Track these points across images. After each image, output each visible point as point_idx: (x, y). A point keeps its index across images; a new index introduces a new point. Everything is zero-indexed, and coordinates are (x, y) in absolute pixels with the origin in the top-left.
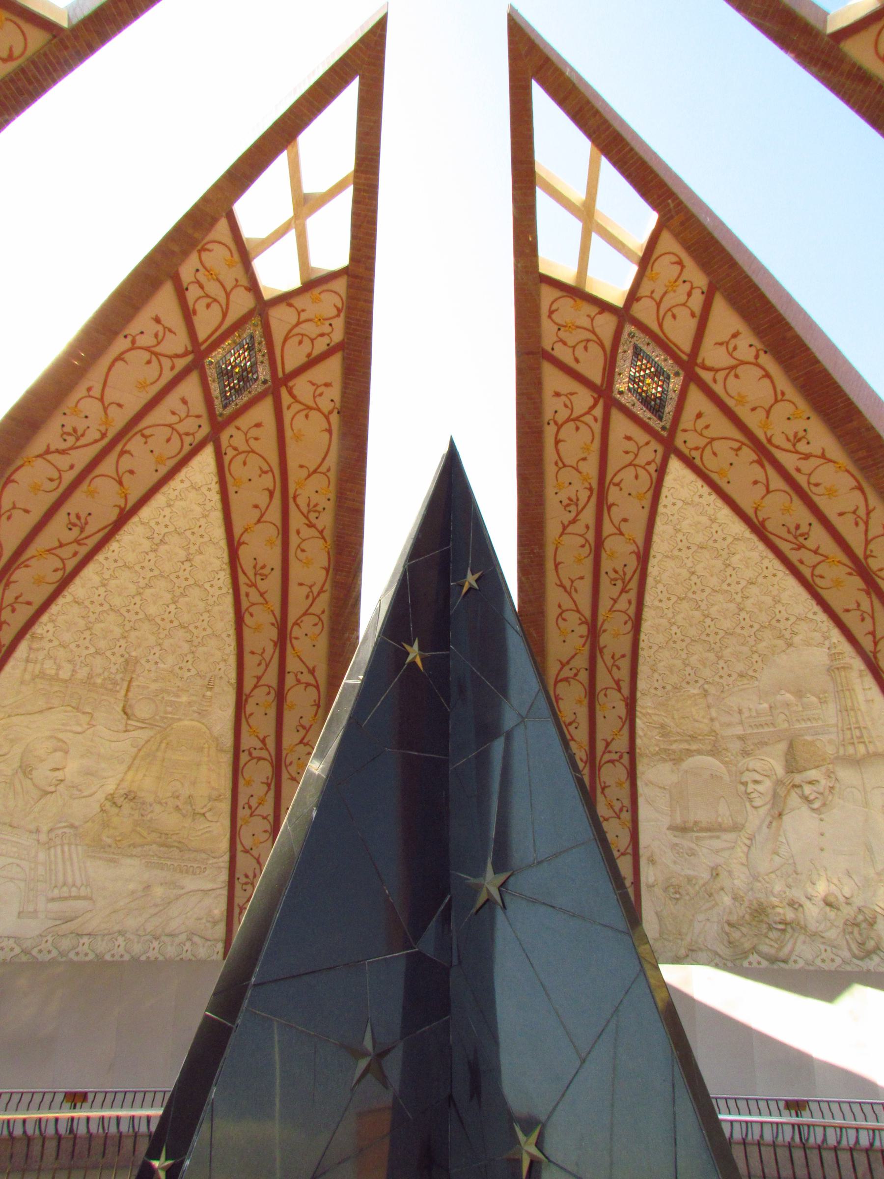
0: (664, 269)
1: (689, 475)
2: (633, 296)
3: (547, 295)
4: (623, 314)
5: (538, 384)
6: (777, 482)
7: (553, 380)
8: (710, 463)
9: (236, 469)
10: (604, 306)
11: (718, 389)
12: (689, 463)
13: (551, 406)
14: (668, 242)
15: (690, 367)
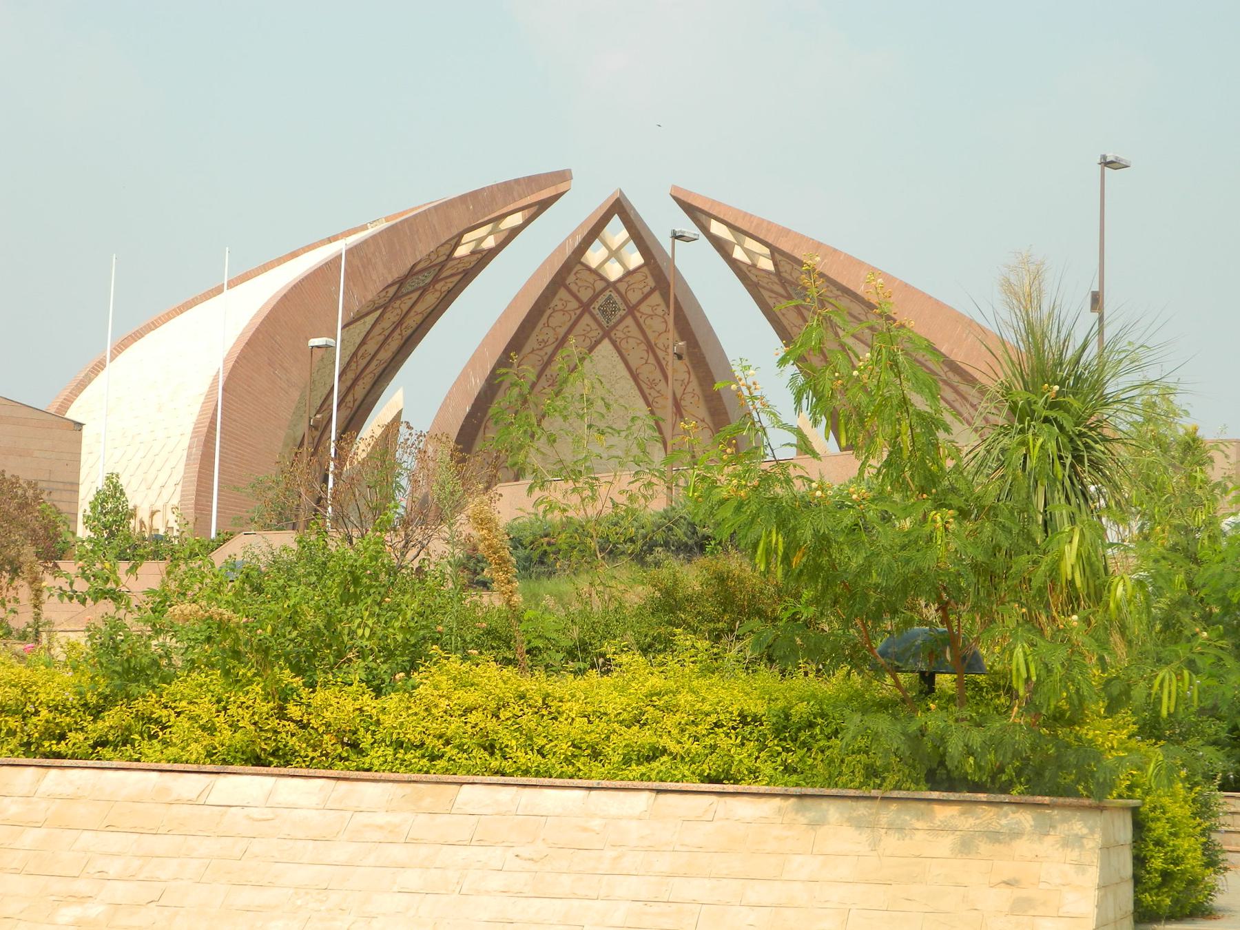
0: (638, 276)
1: (610, 347)
2: (620, 280)
3: (579, 267)
4: (610, 285)
5: (554, 294)
6: (652, 360)
7: (562, 293)
8: (624, 345)
9: (387, 316)
10: (603, 278)
11: (641, 321)
12: (614, 343)
13: (556, 301)
14: (645, 270)
15: (632, 310)
